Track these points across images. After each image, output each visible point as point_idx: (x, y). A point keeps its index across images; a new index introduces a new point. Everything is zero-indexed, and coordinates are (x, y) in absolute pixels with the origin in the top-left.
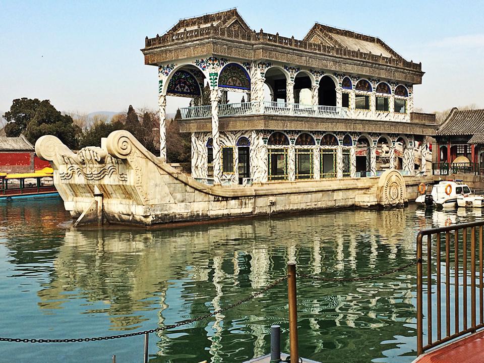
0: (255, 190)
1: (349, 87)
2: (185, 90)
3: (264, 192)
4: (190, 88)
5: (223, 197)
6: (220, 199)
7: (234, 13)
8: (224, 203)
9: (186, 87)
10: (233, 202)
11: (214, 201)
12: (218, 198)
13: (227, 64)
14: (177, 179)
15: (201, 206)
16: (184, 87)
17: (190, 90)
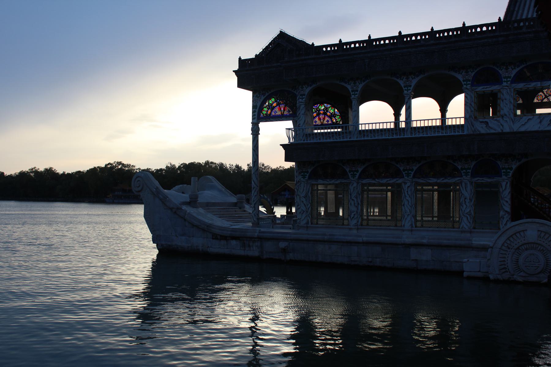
0: (260, 232)
1: (498, 80)
2: (325, 122)
3: (280, 235)
4: (331, 119)
5: (221, 236)
6: (219, 237)
7: (282, 36)
8: (223, 242)
9: (327, 119)
10: (234, 242)
11: (213, 239)
12: (216, 237)
13: (270, 93)
14: (175, 213)
15: (199, 242)
16: (324, 119)
17: (332, 121)
